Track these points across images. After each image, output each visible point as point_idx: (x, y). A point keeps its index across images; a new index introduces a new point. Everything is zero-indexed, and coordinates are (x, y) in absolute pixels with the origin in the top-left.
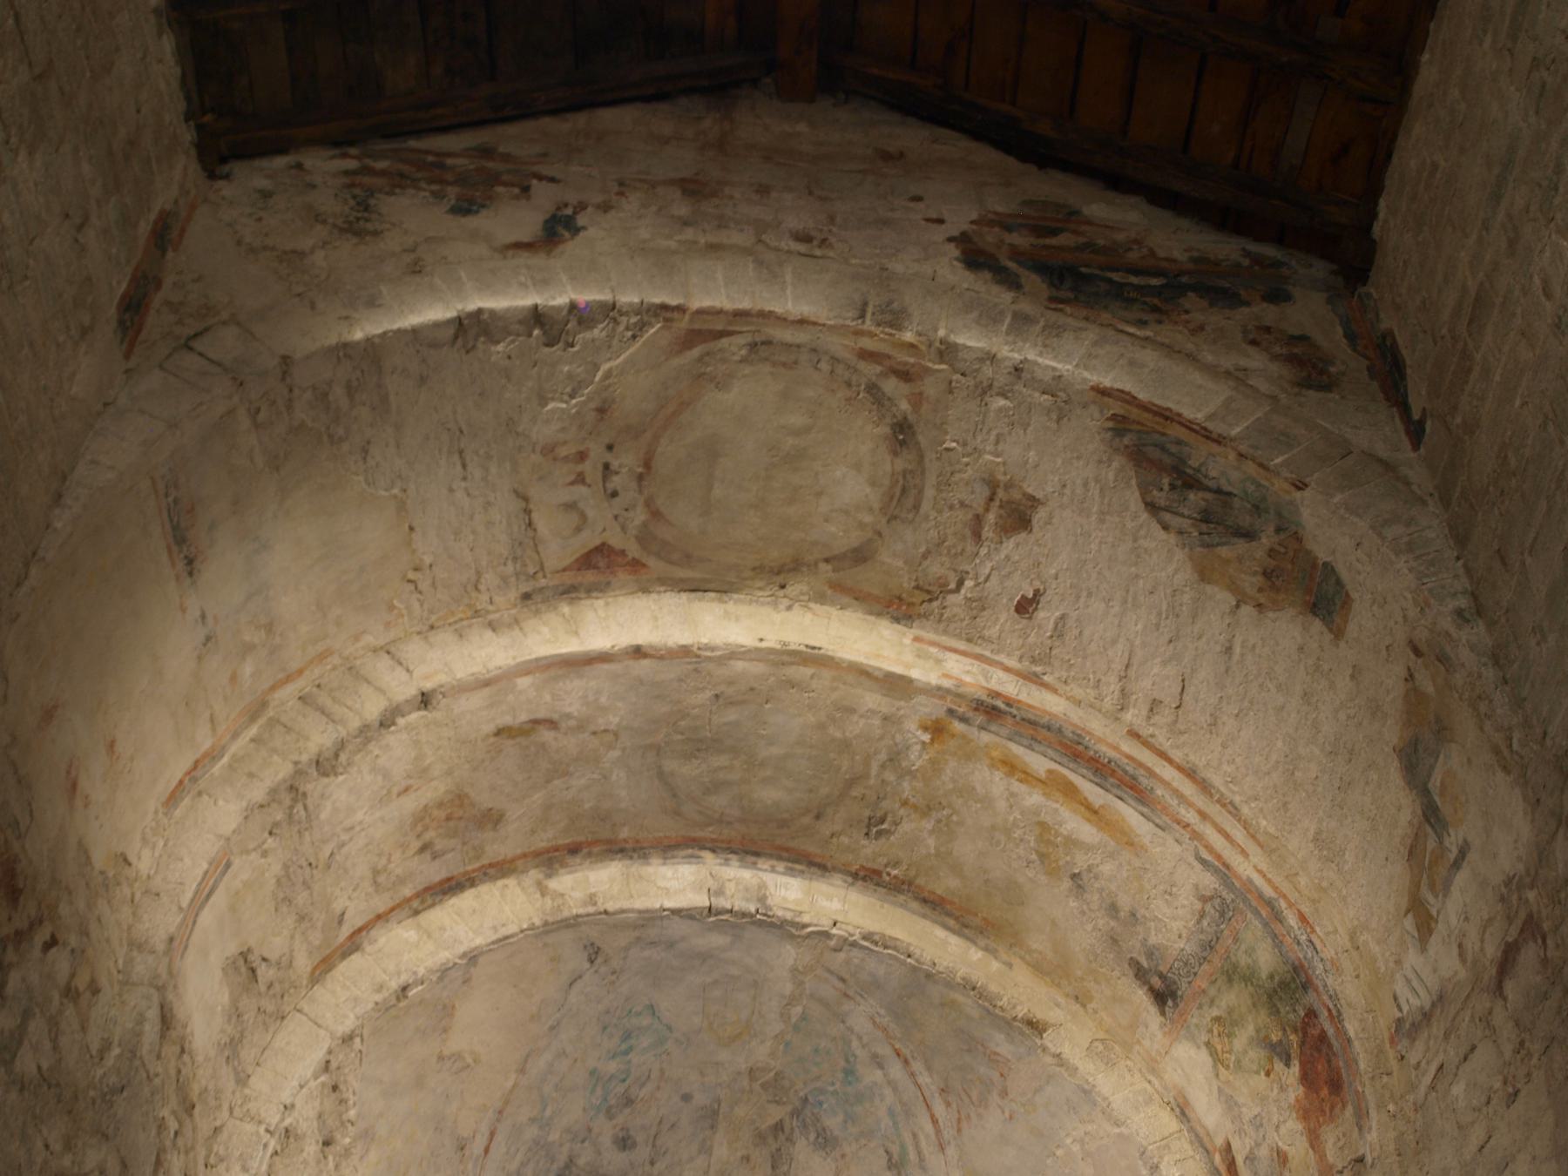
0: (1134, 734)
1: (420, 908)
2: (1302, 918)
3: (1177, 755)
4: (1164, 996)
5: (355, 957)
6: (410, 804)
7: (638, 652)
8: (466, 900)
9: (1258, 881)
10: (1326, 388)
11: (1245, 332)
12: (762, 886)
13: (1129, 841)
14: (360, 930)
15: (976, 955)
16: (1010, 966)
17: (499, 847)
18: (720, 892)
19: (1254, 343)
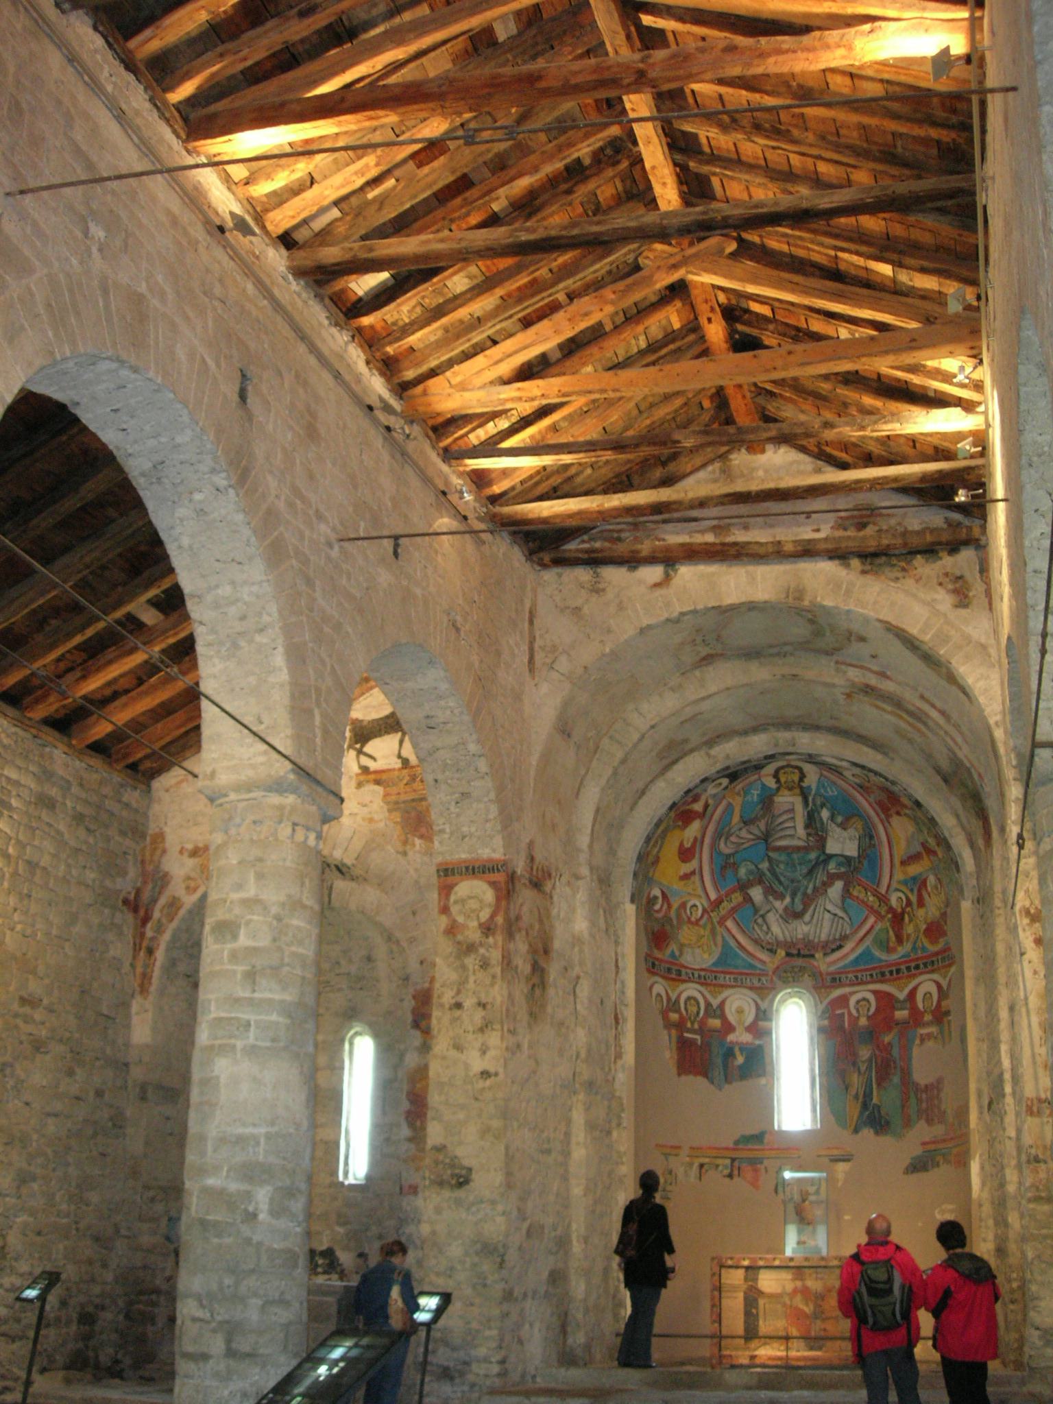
0: (922, 697)
2: (980, 775)
3: (938, 704)
4: (946, 781)
5: (645, 798)
6: (654, 754)
7: (728, 689)
8: (679, 766)
9: (966, 762)
10: (966, 606)
11: (938, 577)
12: (793, 738)
13: (923, 734)
15: (879, 757)
16: (892, 759)
17: (689, 746)
18: (776, 745)
19: (940, 584)
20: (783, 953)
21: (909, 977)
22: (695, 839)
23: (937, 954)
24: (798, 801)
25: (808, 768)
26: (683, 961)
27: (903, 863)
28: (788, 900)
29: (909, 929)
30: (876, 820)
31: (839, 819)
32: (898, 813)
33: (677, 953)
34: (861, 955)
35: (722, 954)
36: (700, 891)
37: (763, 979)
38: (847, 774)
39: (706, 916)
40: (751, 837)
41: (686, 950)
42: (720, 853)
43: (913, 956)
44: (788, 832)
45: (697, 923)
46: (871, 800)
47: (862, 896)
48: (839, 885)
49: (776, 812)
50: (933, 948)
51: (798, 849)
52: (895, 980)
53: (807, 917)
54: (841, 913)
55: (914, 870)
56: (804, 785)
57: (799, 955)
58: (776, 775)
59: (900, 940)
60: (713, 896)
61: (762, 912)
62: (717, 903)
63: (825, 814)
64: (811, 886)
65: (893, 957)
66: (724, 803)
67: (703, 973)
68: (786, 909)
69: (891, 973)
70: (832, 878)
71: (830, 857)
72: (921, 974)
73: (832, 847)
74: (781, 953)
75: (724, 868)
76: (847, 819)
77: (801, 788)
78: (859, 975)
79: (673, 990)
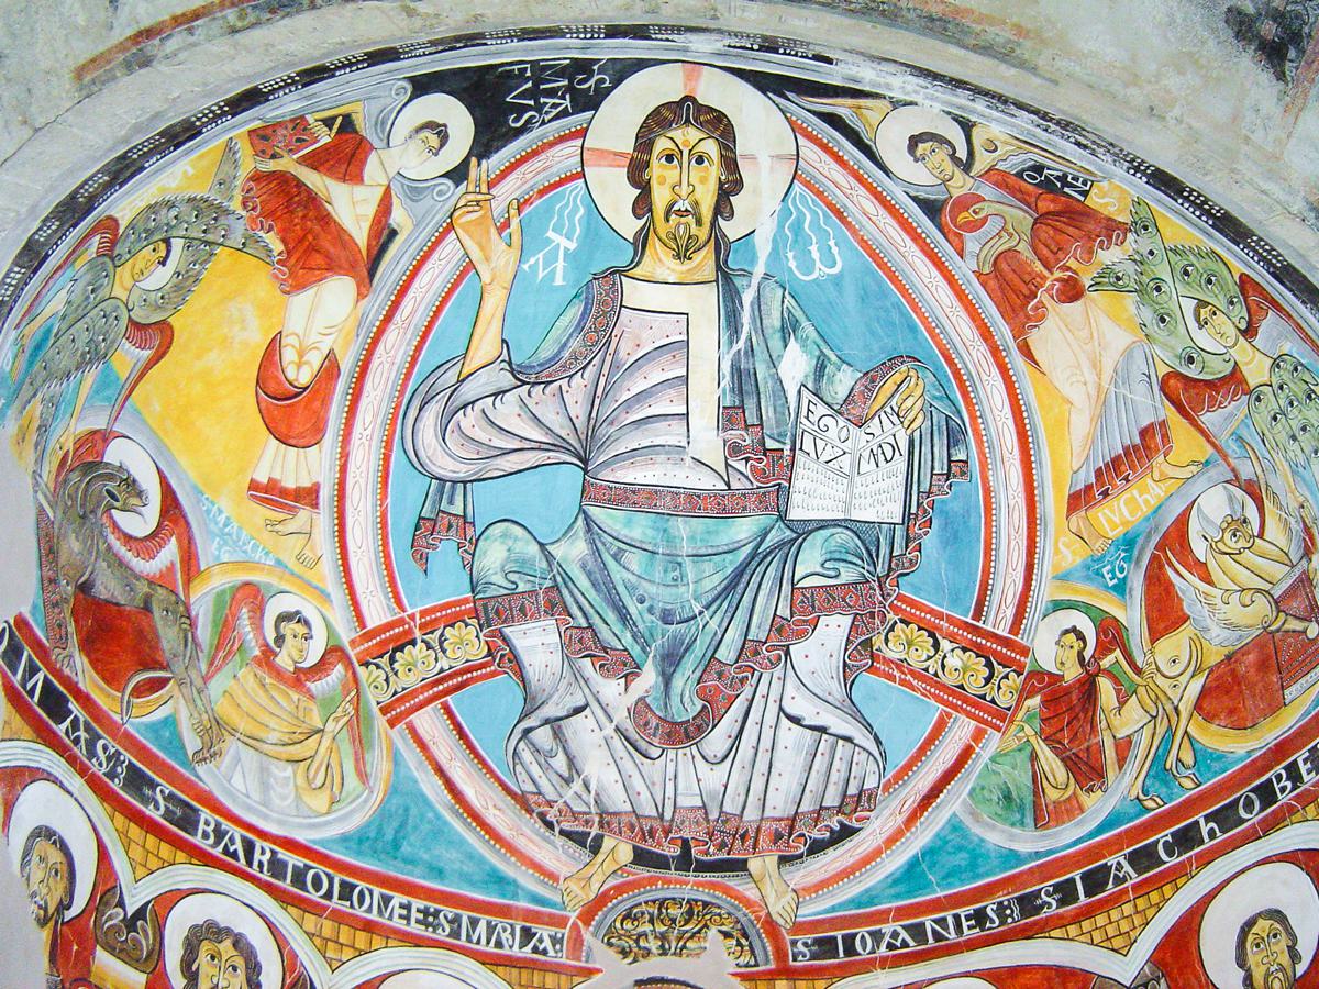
1: (239, 24)
14: (148, 33)
20: (625, 853)
21: (1141, 889)
22: (330, 369)
23: (1281, 749)
24: (704, 303)
25: (755, 117)
26: (208, 777)
27: (1079, 501)
28: (649, 677)
29: (1122, 719)
30: (975, 355)
31: (842, 382)
32: (1072, 291)
33: (192, 743)
34: (929, 852)
35: (383, 814)
36: (327, 573)
37: (544, 932)
38: (891, 139)
39: (339, 669)
40: (536, 434)
41: (231, 747)
42: (418, 465)
43: (1155, 808)
44: (671, 434)
45: (300, 678)
46: (964, 269)
47: (917, 658)
48: (834, 629)
49: (627, 351)
50: (1241, 746)
51: (693, 503)
52: (1088, 913)
53: (716, 741)
54: (839, 724)
55: (1121, 513)
56: (732, 230)
57: (685, 861)
58: (637, 173)
59: (1087, 770)
60: (377, 612)
61: (550, 711)
62: (392, 643)
63: (795, 365)
64: (733, 636)
65: (1067, 837)
66: (450, 246)
67: (293, 860)
68: (640, 709)
69: (1066, 893)
70: (809, 607)
71: (805, 530)
72: (1206, 860)
73: (812, 495)
74: (620, 850)
75: (427, 528)
76: (872, 378)
77: (720, 245)
78: (928, 922)
79: (144, 869)
